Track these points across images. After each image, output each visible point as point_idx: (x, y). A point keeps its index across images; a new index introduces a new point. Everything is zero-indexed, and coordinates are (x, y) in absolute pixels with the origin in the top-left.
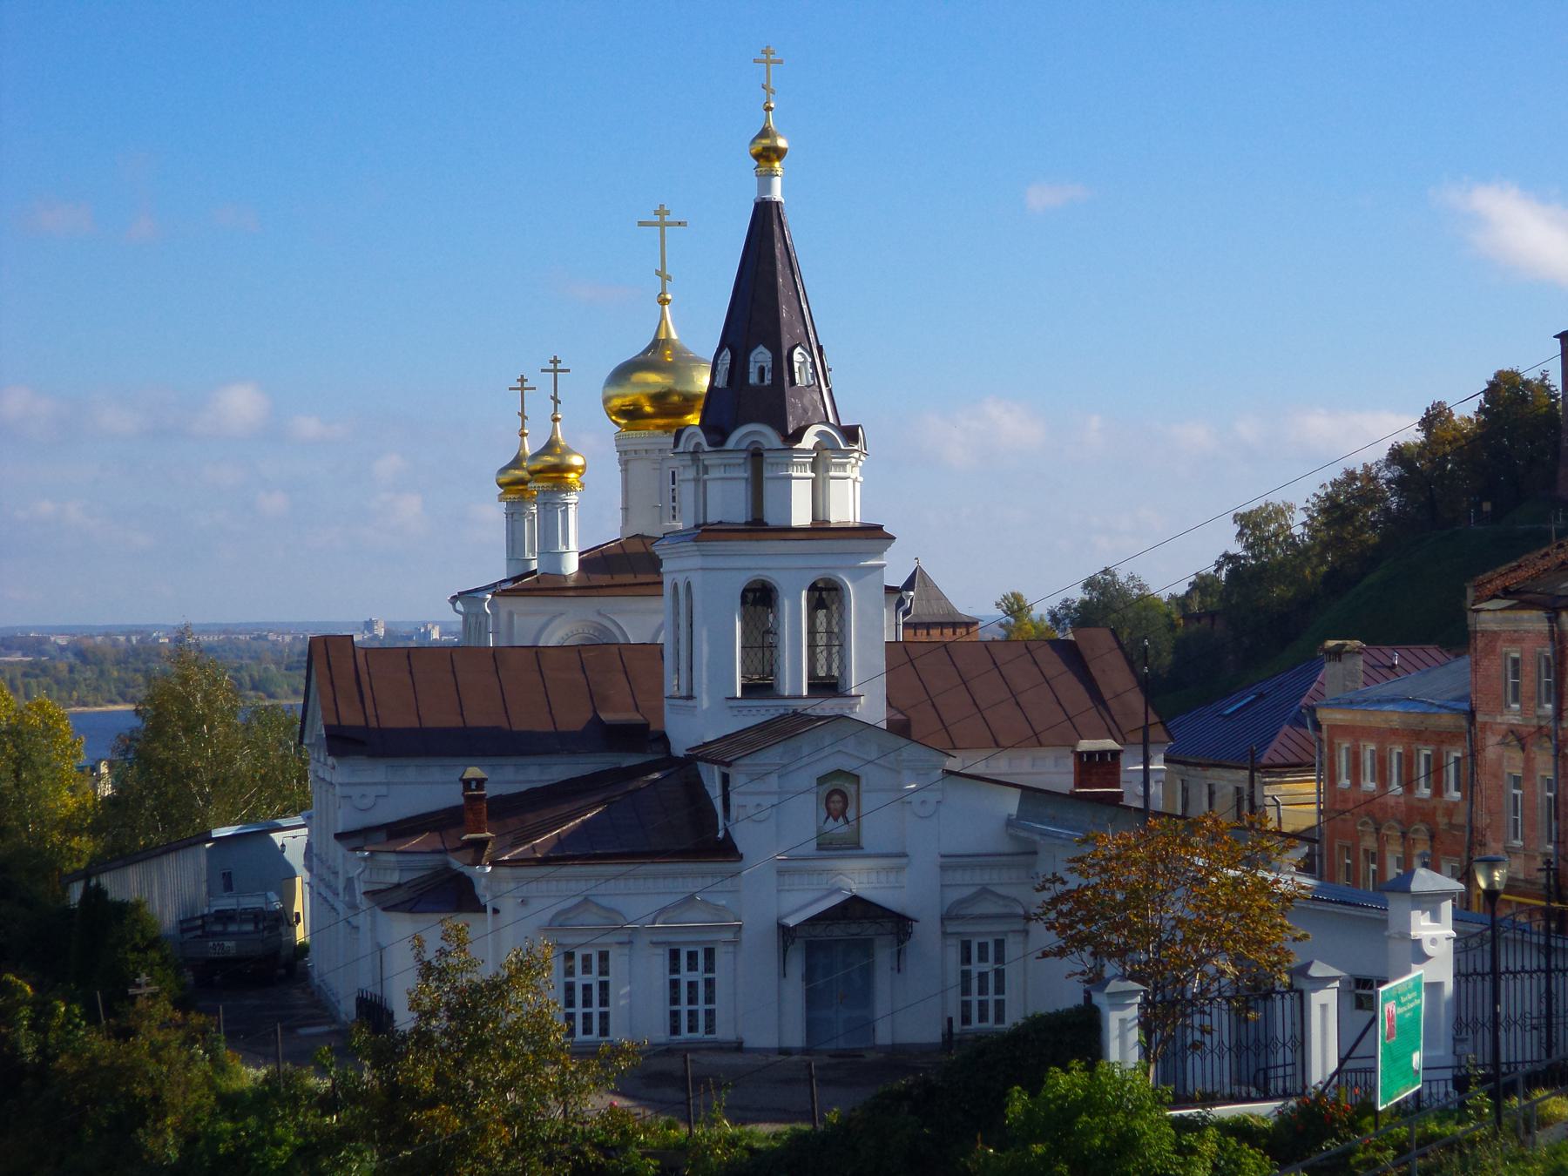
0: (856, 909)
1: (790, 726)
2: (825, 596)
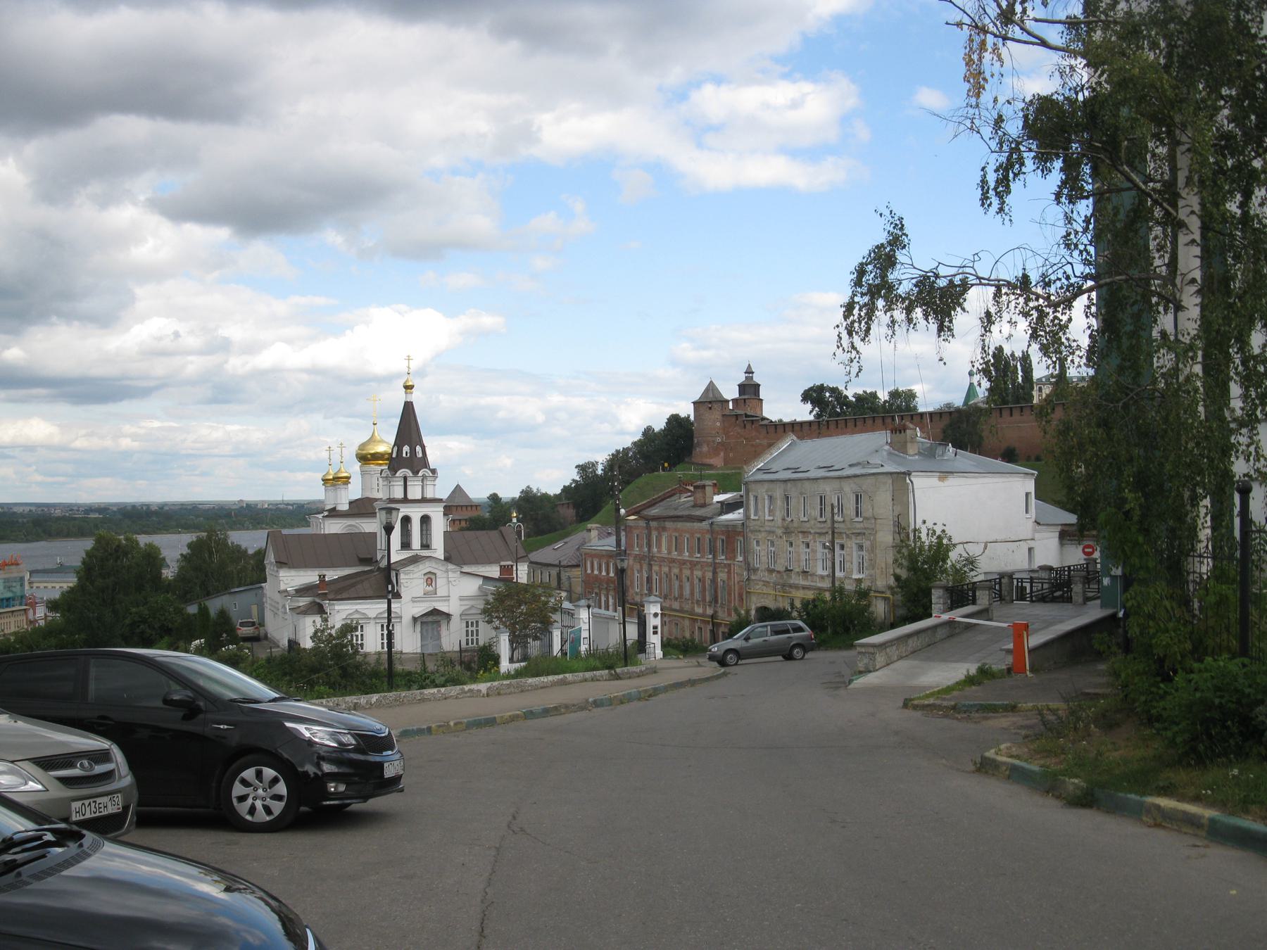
0: (435, 612)
1: (415, 560)
2: (425, 520)
